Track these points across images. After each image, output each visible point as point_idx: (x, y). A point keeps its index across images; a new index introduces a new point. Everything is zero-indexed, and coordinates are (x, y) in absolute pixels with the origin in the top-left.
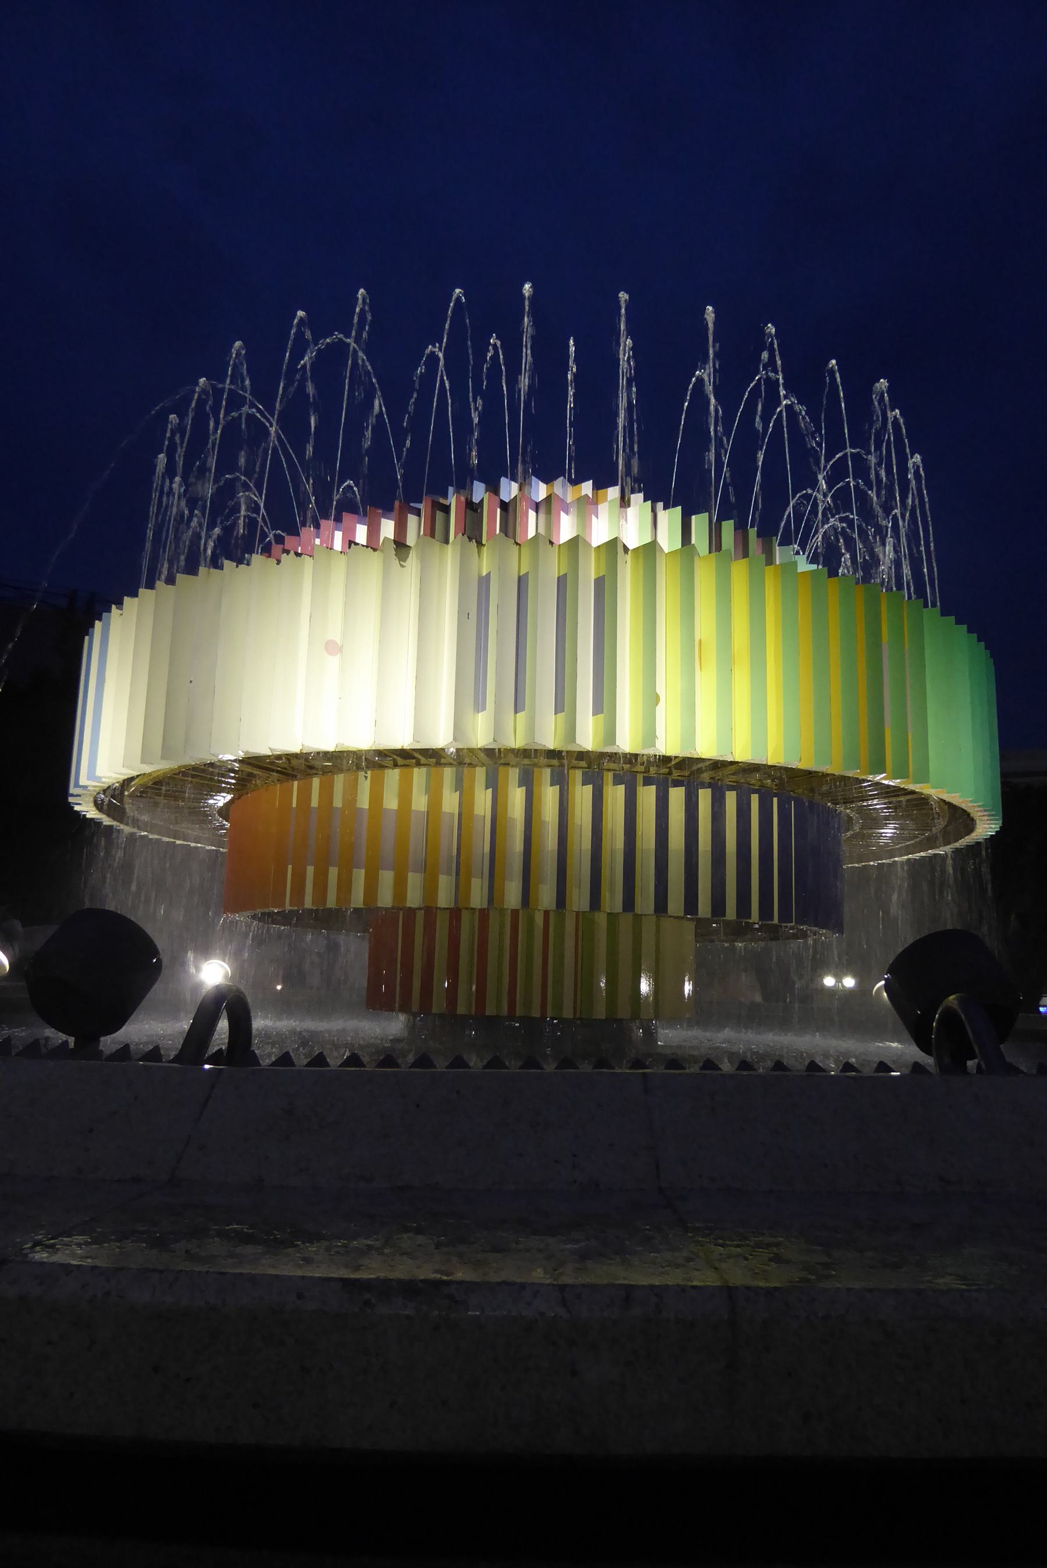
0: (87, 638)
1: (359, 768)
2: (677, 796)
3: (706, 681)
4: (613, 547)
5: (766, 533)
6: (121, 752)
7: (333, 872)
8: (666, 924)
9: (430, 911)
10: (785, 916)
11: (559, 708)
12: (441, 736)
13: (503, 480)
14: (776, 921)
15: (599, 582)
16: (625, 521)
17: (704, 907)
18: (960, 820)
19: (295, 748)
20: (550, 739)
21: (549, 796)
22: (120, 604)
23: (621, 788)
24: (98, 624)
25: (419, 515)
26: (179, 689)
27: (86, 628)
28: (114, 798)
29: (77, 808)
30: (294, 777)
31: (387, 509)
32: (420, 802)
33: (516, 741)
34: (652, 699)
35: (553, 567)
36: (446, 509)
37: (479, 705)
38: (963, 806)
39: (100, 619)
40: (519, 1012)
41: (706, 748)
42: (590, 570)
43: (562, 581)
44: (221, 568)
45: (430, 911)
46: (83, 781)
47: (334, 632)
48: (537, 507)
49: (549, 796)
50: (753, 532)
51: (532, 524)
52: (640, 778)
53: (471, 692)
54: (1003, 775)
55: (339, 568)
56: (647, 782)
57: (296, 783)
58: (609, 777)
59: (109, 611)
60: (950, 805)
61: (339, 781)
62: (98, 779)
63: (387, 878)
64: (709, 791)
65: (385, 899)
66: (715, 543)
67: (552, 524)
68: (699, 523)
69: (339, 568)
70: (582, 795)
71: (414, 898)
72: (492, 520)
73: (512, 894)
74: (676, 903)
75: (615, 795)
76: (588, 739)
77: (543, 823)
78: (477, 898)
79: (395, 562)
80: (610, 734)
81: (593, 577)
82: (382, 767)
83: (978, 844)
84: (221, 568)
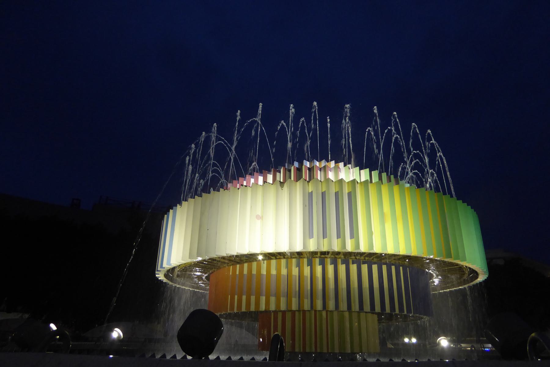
0: (166, 216)
1: (291, 258)
2: (375, 268)
3: (388, 226)
4: (354, 181)
5: (396, 177)
6: (181, 255)
7: (244, 297)
8: (363, 315)
9: (276, 312)
10: (409, 311)
11: (338, 237)
12: (299, 248)
13: (304, 161)
14: (405, 313)
15: (349, 194)
16: (348, 173)
17: (378, 309)
18: (474, 274)
19: (235, 254)
20: (336, 248)
21: (330, 269)
22: (180, 204)
23: (355, 265)
24: (171, 211)
25: (280, 173)
26: (202, 232)
27: (167, 212)
28: (170, 272)
29: (157, 276)
30: (238, 263)
31: (269, 171)
32: (284, 272)
33: (325, 248)
34: (370, 233)
35: (334, 189)
36: (290, 171)
37: (311, 236)
38: (476, 270)
39: (172, 209)
40: (318, 351)
41: (391, 250)
42: (346, 190)
43: (337, 194)
44: (219, 191)
45: (300, 310)
46: (165, 265)
47: (259, 213)
48: (320, 170)
49: (330, 269)
50: (392, 176)
51: (319, 175)
52: (351, 261)
53: (308, 233)
54: (487, 259)
55: (272, 191)
56: (364, 263)
57: (238, 266)
58: (339, 261)
59: (176, 206)
60: (470, 268)
61: (246, 265)
62: (170, 265)
63: (273, 299)
64: (376, 265)
65: (263, 308)
66: (389, 180)
67: (326, 174)
68: (375, 174)
69: (260, 191)
70: (342, 268)
71: (283, 307)
72: (305, 174)
73: (319, 305)
74: (367, 307)
75: (354, 268)
76: (350, 248)
77: (328, 278)
78: (307, 306)
79: (280, 188)
80: (357, 245)
81: (347, 192)
82: (271, 259)
83: (477, 284)
84: (219, 191)
